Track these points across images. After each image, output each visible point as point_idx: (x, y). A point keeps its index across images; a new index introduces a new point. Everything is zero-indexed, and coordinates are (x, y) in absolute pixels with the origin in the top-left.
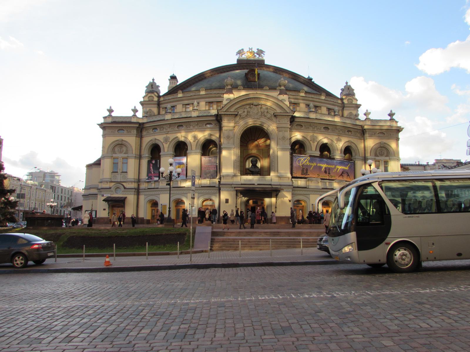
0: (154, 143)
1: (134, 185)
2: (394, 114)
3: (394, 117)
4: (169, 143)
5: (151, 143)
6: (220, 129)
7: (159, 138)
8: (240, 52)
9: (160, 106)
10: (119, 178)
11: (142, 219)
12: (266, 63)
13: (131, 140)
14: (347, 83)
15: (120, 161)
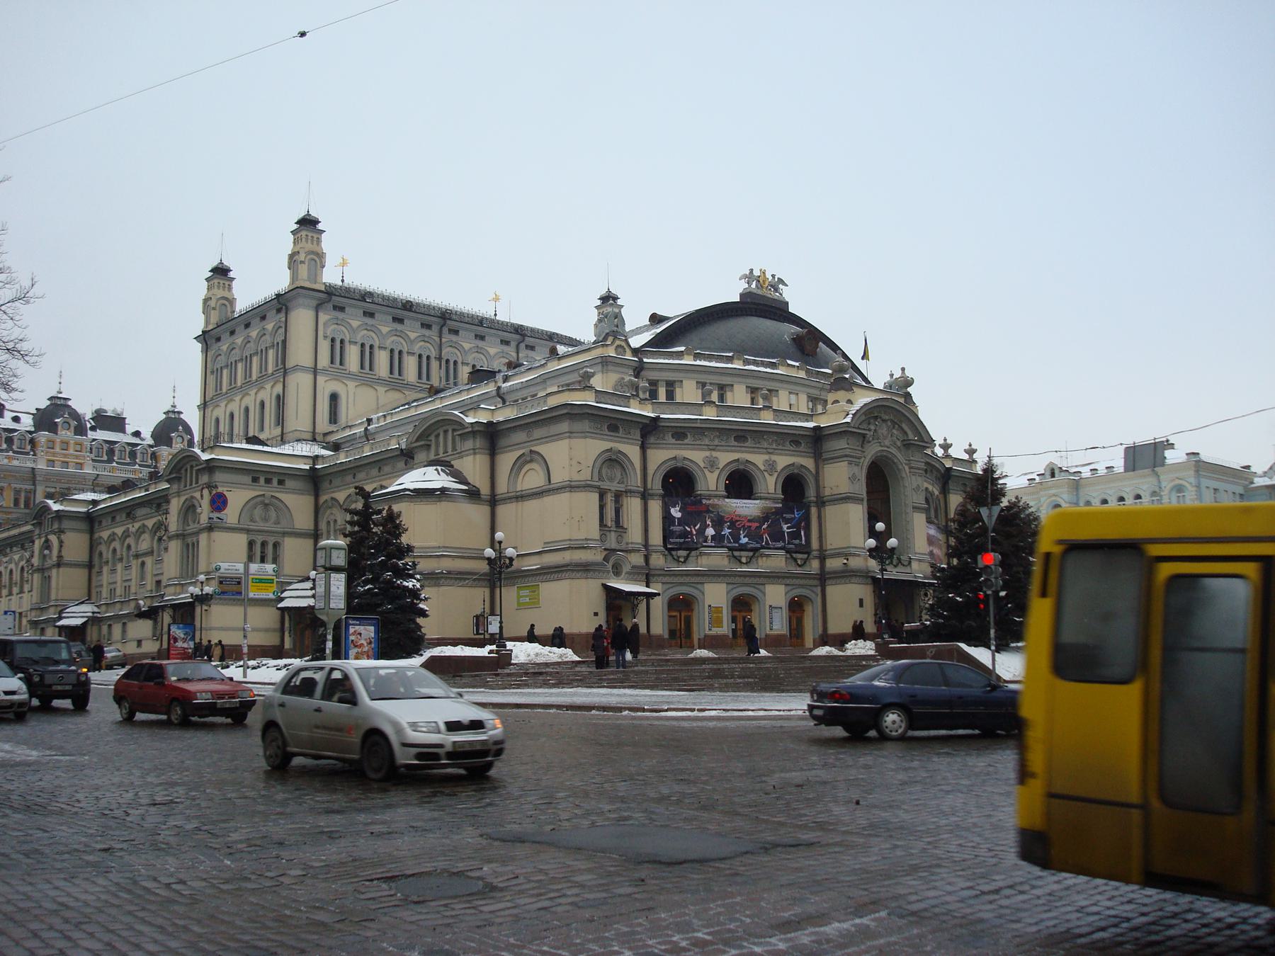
0: (679, 465)
1: (637, 559)
2: (974, 451)
3: (975, 456)
4: (717, 472)
5: (671, 464)
6: (819, 456)
7: (695, 456)
8: (749, 277)
9: (643, 373)
10: (612, 542)
11: (659, 638)
12: (792, 309)
13: (632, 451)
14: (892, 375)
15: (609, 498)
